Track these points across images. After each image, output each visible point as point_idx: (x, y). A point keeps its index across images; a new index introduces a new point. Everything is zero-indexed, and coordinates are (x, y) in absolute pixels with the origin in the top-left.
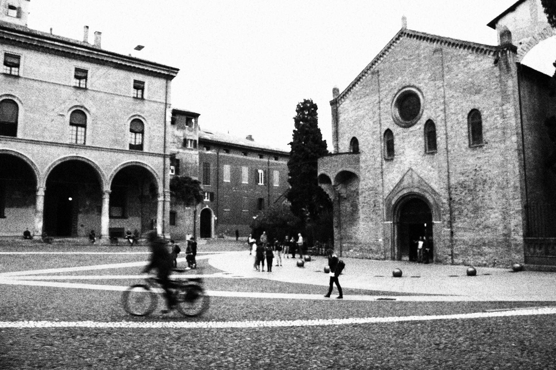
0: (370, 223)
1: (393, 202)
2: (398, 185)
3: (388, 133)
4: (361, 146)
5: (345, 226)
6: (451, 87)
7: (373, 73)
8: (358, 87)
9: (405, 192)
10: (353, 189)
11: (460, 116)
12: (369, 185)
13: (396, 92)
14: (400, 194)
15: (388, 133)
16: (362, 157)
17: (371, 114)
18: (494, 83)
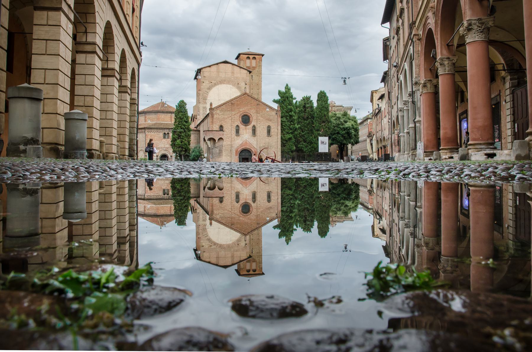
0: (228, 157)
1: (239, 150)
2: (241, 145)
3: (238, 126)
4: (224, 129)
5: (215, 158)
6: (262, 117)
7: (232, 104)
8: (224, 107)
9: (244, 147)
10: (220, 144)
11: (264, 127)
12: (228, 143)
13: (242, 113)
14: (242, 148)
15: (238, 126)
16: (225, 133)
17: (230, 118)
18: (276, 120)
